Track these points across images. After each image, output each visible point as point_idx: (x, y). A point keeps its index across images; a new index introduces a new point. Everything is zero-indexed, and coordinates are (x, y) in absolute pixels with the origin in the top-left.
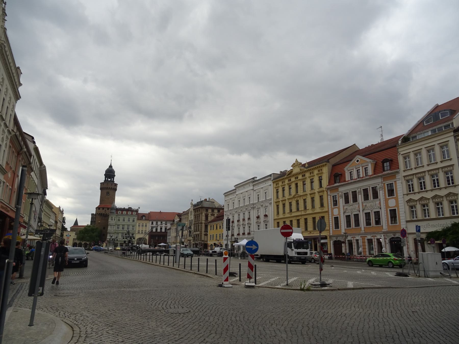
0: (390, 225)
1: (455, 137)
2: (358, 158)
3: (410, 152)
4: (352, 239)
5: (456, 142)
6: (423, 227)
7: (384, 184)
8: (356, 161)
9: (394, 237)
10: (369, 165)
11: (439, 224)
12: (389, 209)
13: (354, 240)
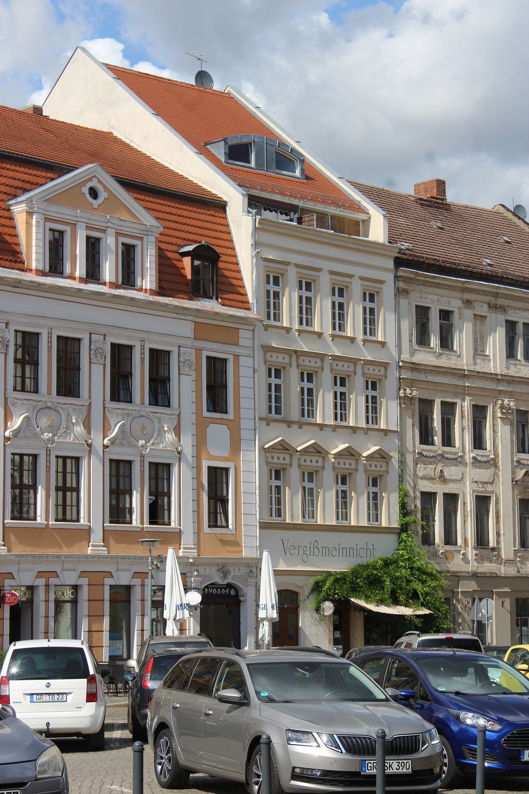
0: (206, 529)
1: (396, 277)
2: (99, 181)
3: (287, 264)
4: (137, 582)
5: (395, 295)
6: (301, 552)
7: (199, 351)
8: (85, 190)
9: (220, 581)
10: (145, 238)
11: (341, 547)
12: (205, 464)
13: (47, 585)
